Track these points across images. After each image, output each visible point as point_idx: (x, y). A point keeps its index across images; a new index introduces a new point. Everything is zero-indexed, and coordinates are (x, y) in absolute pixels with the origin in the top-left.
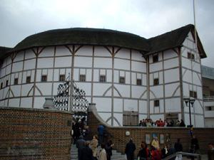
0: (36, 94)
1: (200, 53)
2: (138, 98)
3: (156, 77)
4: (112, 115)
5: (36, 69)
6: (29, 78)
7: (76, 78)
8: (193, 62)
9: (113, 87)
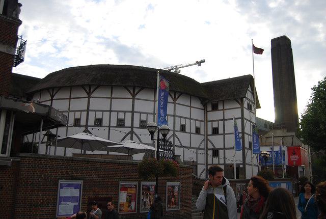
5: (88, 110)
7: (137, 123)
8: (251, 114)
9: (174, 135)
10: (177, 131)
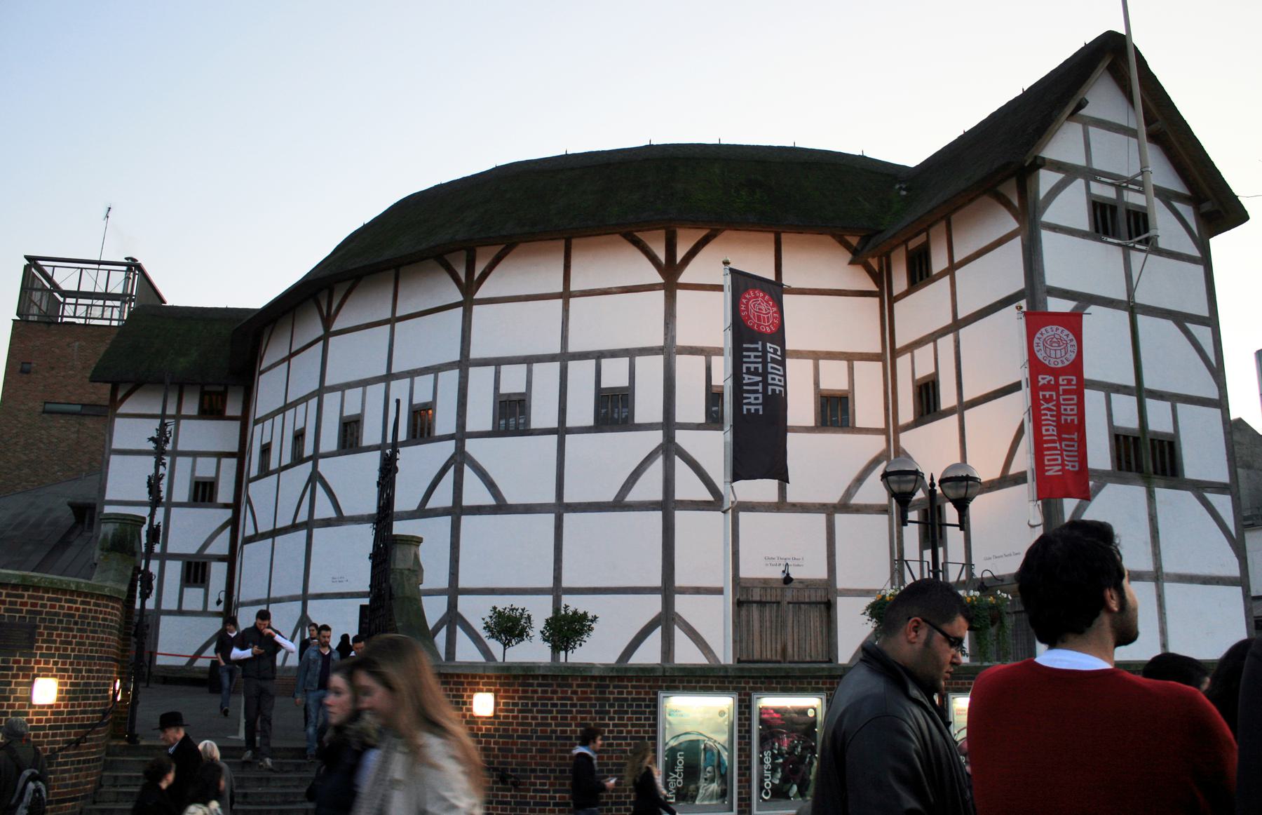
0: (317, 516)
1: (1195, 199)
2: (834, 498)
3: (924, 370)
4: (668, 604)
6: (299, 436)
7: (481, 415)
8: (1137, 258)
9: (669, 449)
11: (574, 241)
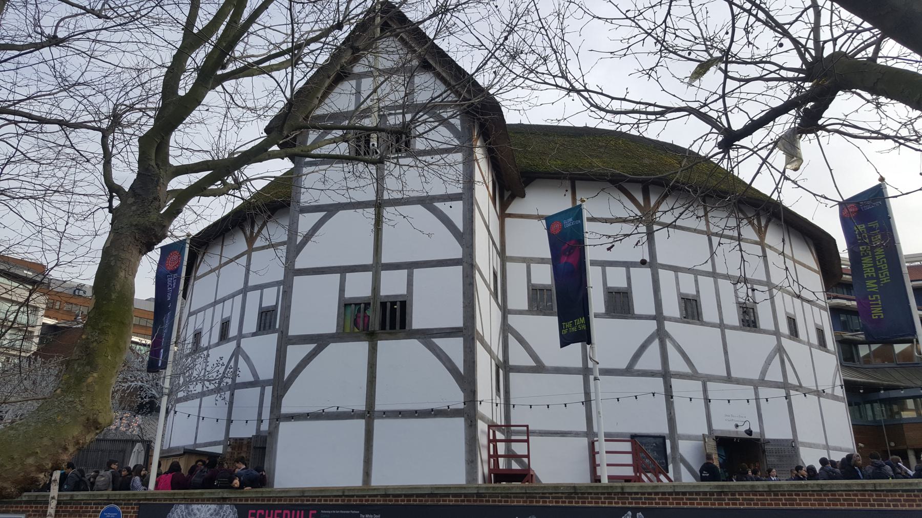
9: (661, 335)
10: (670, 319)
11: (577, 183)
